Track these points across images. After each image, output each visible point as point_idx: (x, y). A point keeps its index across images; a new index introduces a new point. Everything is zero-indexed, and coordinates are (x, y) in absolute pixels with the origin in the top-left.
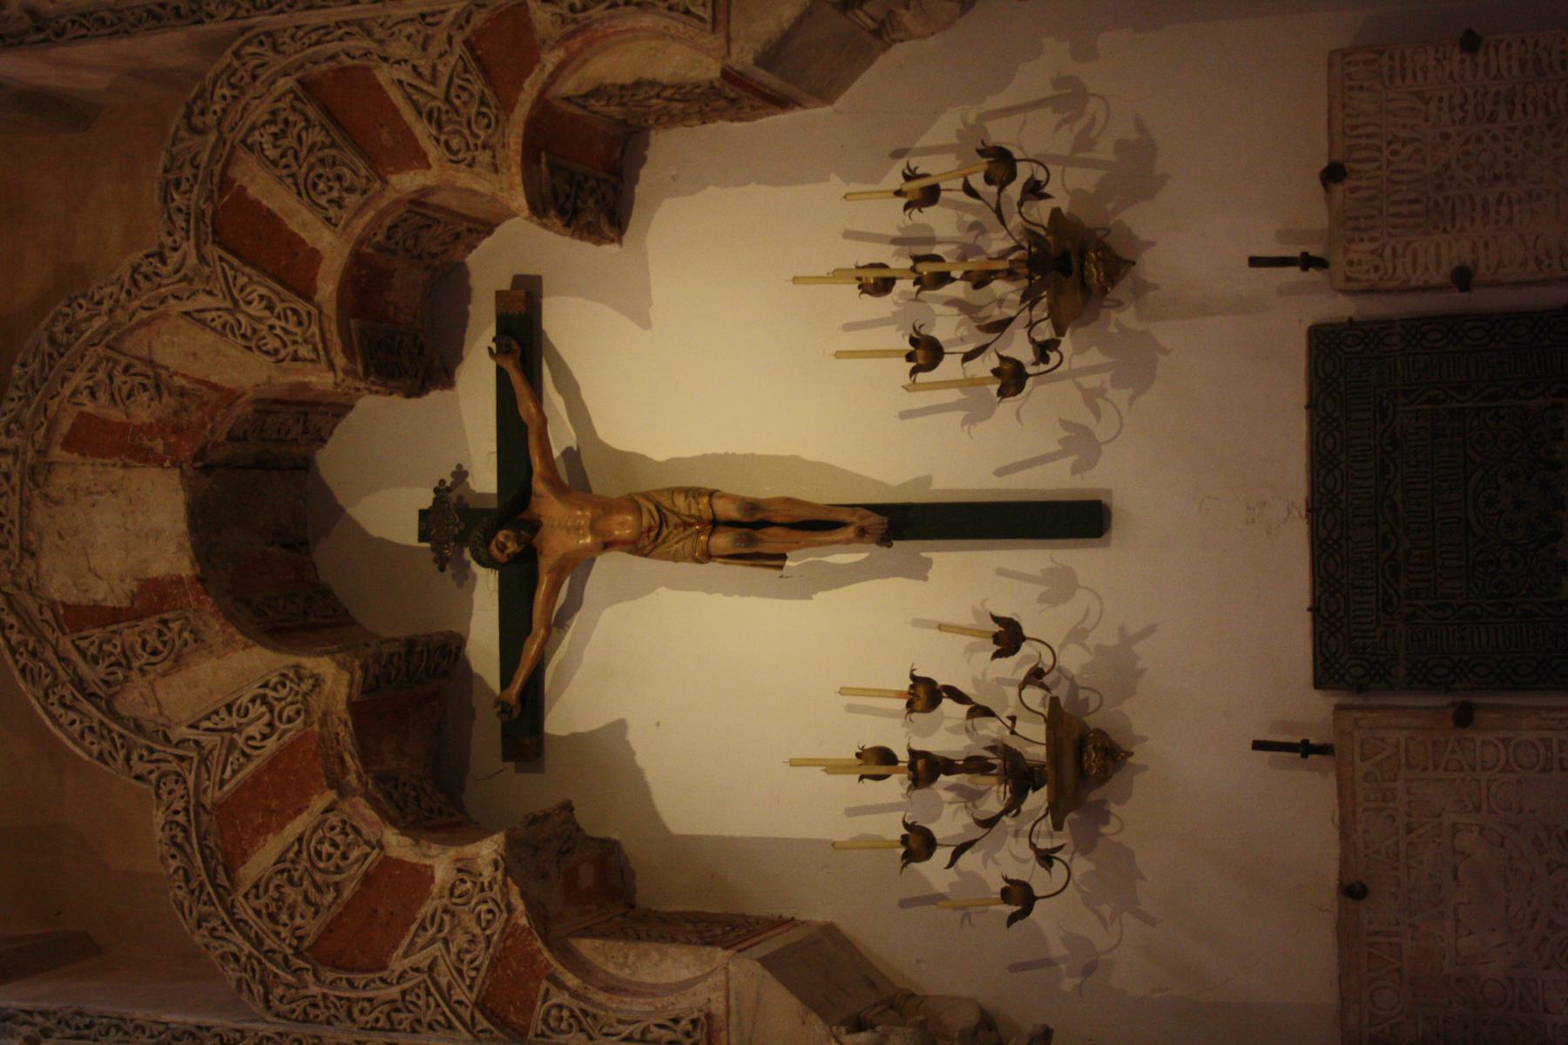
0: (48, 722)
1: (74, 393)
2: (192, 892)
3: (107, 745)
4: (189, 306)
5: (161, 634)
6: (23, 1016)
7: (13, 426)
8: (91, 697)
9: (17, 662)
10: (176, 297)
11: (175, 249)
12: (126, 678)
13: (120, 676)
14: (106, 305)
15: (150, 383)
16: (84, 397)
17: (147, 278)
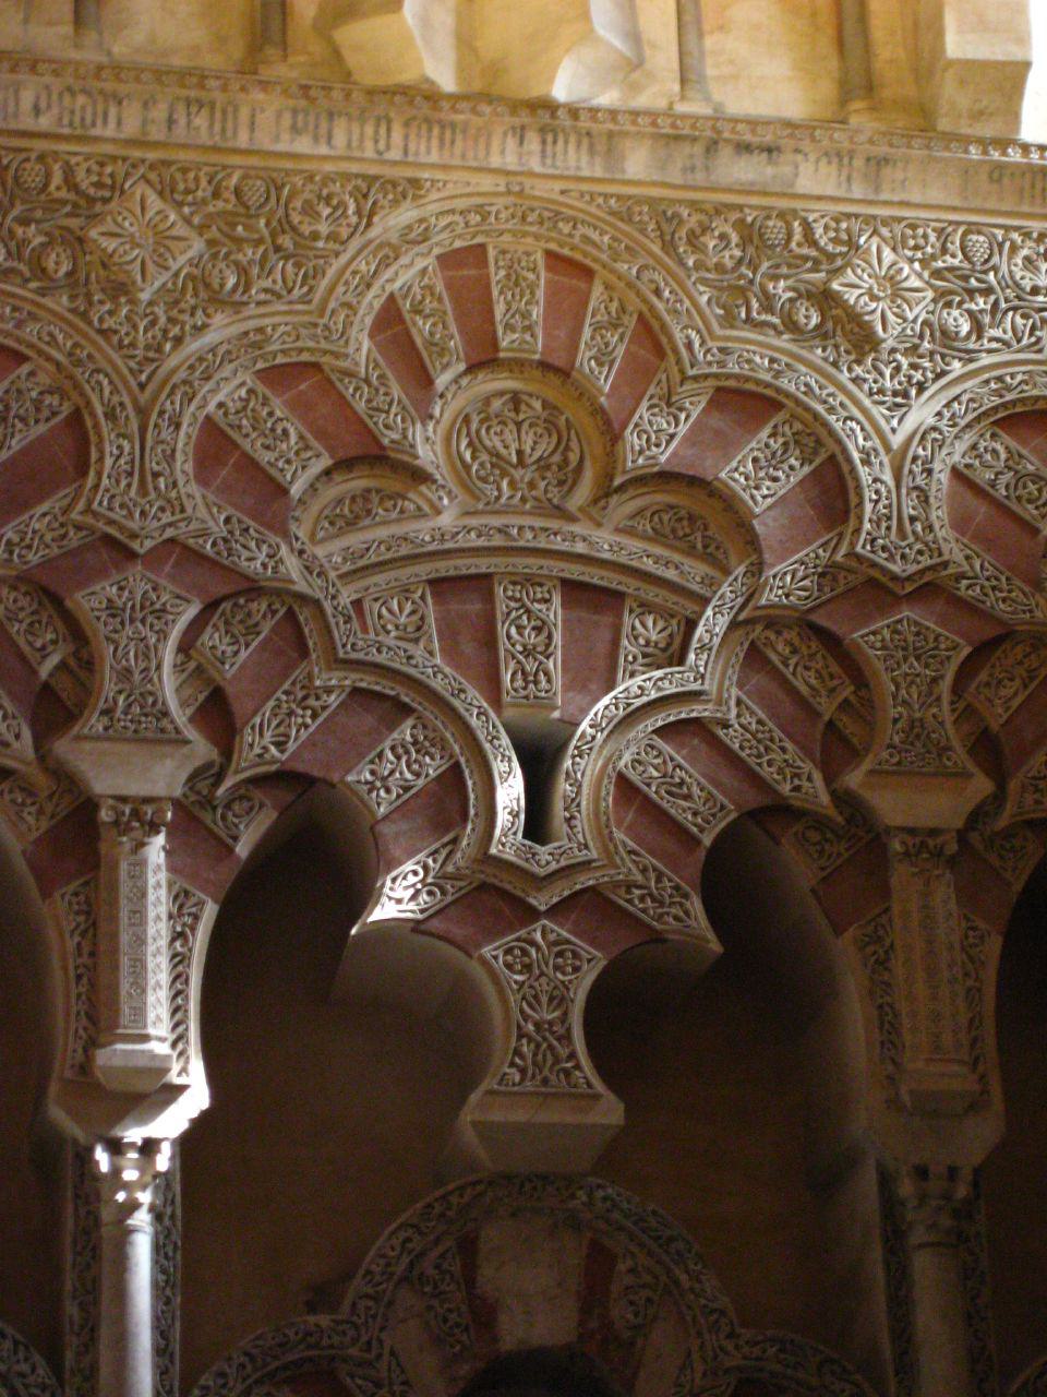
0: (394, 1226)
1: (633, 1255)
2: (270, 1348)
3: (378, 1278)
4: (696, 1357)
5: (458, 1325)
6: (170, 1197)
7: (609, 1203)
8: (412, 1264)
9: (436, 1200)
10: (702, 1346)
11: (737, 1347)
12: (425, 1293)
13: (426, 1290)
14: (697, 1286)
15: (640, 1320)
16: (629, 1263)
17: (717, 1321)
